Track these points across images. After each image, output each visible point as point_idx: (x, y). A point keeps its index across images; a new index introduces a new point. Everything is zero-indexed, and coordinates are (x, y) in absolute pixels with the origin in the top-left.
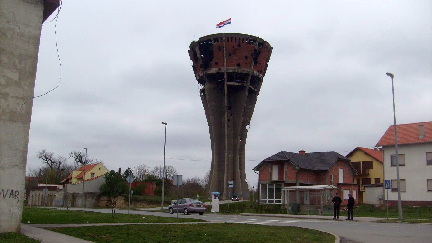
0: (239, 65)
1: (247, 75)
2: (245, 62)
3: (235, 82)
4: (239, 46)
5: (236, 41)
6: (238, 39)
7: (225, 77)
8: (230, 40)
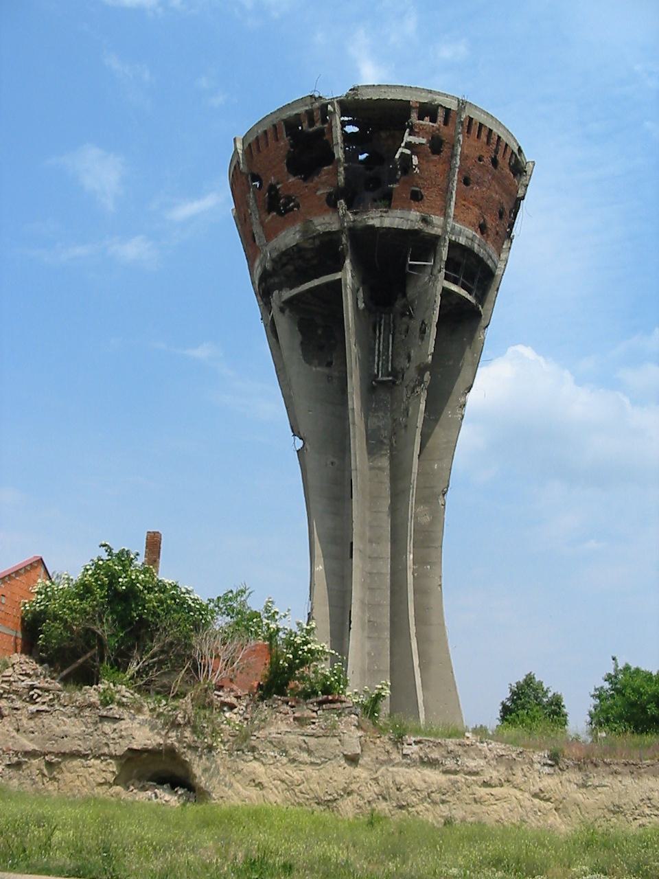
3: (464, 287)
5: (488, 143)
8: (475, 129)
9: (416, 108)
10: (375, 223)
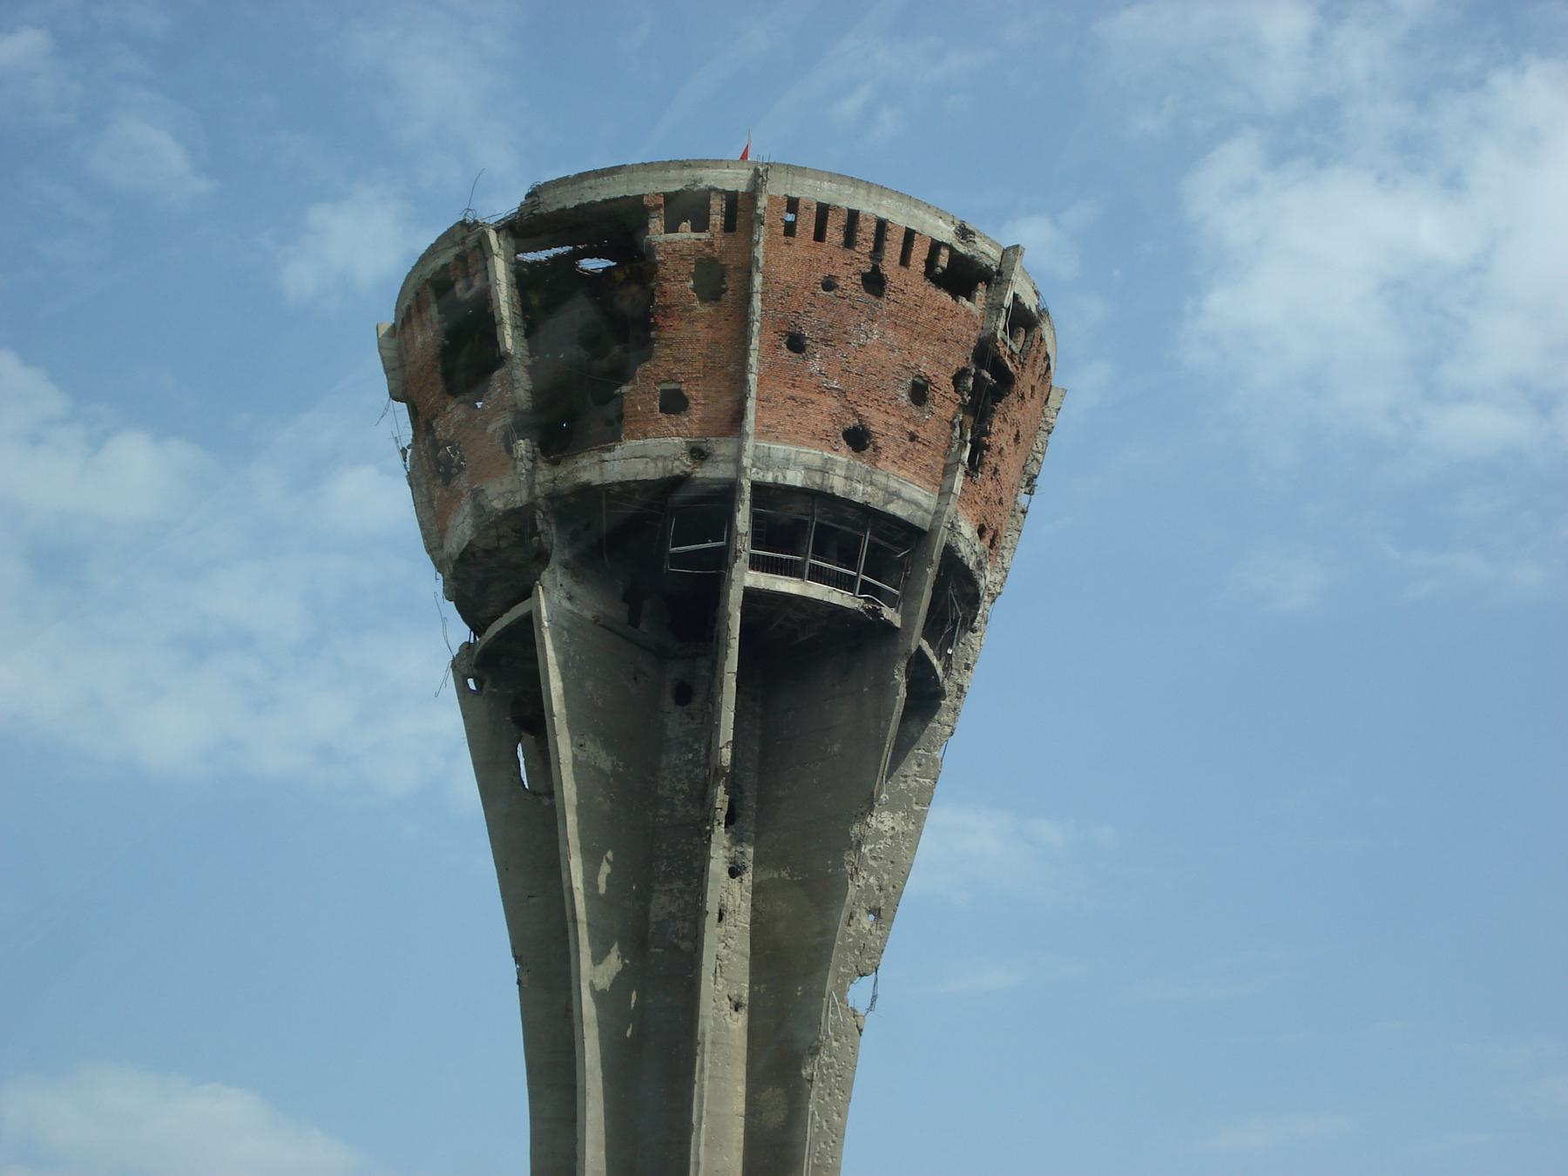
0: (858, 439)
1: (910, 536)
2: (911, 428)
3: (818, 575)
4: (874, 282)
5: (850, 241)
6: (867, 231)
7: (743, 519)
9: (658, 207)
10: (592, 479)
